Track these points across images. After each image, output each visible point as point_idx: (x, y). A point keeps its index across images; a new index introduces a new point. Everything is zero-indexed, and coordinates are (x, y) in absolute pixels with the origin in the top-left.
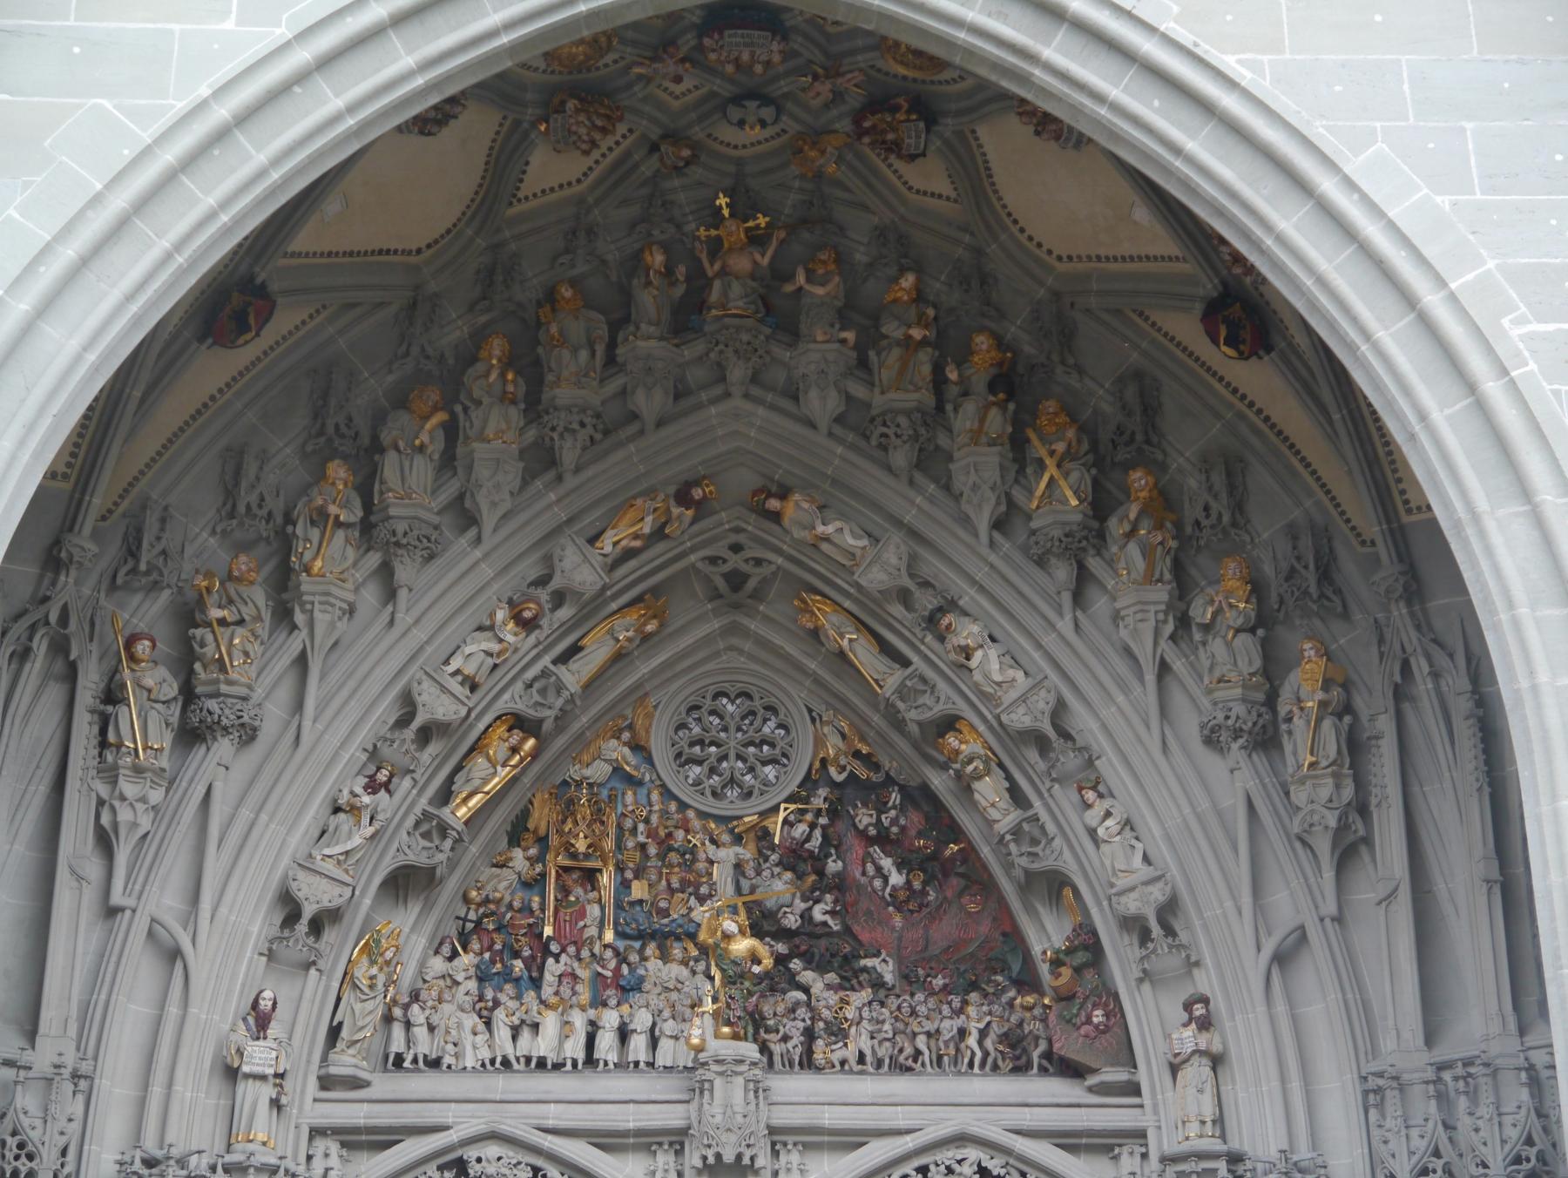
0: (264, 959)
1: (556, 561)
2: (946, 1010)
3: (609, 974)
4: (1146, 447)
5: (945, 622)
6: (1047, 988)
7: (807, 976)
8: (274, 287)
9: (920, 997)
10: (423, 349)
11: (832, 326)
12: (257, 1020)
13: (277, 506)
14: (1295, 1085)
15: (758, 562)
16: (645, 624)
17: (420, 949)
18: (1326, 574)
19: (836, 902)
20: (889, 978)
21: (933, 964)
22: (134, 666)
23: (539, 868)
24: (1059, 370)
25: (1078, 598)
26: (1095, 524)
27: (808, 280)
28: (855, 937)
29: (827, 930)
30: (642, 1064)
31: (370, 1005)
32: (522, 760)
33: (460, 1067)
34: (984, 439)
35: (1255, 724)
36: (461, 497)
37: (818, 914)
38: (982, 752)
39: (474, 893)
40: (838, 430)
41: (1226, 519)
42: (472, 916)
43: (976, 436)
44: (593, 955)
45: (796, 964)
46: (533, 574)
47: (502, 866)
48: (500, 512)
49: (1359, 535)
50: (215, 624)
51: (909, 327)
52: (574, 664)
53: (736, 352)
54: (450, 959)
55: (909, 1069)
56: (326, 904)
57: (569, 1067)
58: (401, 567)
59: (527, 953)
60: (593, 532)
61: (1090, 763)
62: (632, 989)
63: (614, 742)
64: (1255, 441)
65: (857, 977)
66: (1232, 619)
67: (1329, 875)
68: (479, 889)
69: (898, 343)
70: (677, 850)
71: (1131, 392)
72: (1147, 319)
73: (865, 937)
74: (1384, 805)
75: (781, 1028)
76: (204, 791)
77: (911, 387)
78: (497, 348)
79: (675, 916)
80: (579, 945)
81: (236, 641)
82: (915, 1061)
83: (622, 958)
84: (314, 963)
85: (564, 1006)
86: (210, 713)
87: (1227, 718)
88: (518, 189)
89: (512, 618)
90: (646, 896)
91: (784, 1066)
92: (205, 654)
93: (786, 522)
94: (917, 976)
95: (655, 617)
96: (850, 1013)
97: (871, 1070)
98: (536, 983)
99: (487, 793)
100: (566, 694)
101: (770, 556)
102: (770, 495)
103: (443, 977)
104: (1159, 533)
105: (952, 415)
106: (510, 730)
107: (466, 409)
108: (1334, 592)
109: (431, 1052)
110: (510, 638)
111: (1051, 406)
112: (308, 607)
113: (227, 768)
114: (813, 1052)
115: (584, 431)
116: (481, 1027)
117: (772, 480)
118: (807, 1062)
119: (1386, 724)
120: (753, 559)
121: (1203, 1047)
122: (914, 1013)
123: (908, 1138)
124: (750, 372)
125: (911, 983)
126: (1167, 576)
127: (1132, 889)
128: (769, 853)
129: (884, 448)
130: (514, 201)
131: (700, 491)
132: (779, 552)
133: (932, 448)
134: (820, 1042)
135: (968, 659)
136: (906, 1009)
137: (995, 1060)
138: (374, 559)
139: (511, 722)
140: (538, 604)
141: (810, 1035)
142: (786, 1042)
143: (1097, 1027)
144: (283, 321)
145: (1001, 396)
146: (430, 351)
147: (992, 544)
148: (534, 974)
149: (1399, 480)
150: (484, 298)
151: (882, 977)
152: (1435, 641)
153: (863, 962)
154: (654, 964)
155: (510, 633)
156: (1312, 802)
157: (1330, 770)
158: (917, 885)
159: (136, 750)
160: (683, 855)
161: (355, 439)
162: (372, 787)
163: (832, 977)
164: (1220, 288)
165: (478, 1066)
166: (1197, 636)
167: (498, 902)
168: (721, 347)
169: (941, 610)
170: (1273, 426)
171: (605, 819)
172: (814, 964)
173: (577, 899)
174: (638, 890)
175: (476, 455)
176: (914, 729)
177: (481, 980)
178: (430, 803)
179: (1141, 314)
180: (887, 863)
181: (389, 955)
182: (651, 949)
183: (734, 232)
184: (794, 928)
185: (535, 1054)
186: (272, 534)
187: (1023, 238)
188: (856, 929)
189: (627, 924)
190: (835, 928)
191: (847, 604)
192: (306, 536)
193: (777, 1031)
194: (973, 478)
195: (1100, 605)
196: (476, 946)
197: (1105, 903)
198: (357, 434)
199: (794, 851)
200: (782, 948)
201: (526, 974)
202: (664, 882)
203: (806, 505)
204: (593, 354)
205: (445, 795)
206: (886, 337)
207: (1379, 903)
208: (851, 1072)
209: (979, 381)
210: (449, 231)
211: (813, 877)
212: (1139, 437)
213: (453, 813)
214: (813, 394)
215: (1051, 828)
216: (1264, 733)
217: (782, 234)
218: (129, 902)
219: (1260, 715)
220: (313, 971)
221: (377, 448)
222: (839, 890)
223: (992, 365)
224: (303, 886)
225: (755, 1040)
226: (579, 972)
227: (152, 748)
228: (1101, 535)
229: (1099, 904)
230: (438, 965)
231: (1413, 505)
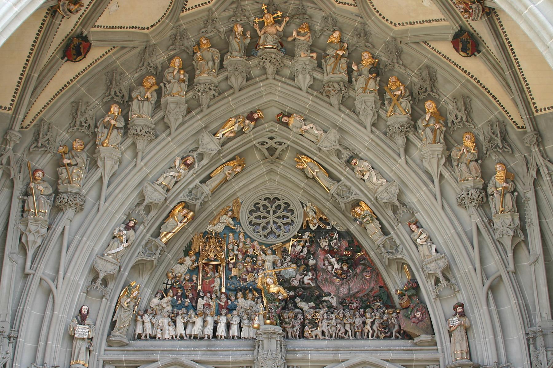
0: (85, 294)
1: (200, 140)
2: (357, 315)
3: (223, 304)
4: (431, 93)
5: (354, 161)
6: (398, 306)
7: (302, 304)
8: (91, 38)
9: (347, 310)
10: (149, 64)
11: (307, 51)
12: (81, 318)
13: (92, 123)
14: (500, 337)
15: (280, 143)
16: (236, 168)
17: (148, 294)
18: (504, 139)
19: (313, 275)
20: (334, 304)
21: (352, 299)
22: (35, 181)
23: (196, 264)
24: (397, 65)
25: (406, 151)
26: (413, 123)
27: (298, 35)
30: (235, 337)
31: (126, 314)
32: (188, 220)
33: (163, 339)
34: (367, 91)
35: (479, 196)
36: (163, 118)
37: (306, 280)
38: (370, 214)
39: (170, 274)
40: (310, 90)
41: (464, 119)
42: (170, 282)
43: (364, 90)
44: (217, 297)
45: (298, 300)
46: (191, 148)
47: (181, 264)
48: (178, 124)
49: (517, 124)
50: (67, 165)
51: (338, 50)
52: (208, 182)
53: (270, 61)
54: (161, 299)
55: (343, 338)
56: (108, 273)
57: (206, 338)
58: (140, 144)
59: (191, 296)
60: (215, 132)
61: (413, 214)
62: (233, 310)
63: (225, 217)
64: (475, 91)
65: (322, 304)
66: (469, 157)
67: (510, 255)
68: (172, 273)
69: (333, 57)
70: (250, 256)
71: (425, 73)
72: (430, 46)
73: (325, 289)
74: (532, 226)
75: (291, 322)
76: (62, 229)
77: (338, 72)
78: (177, 62)
79: (249, 282)
80: (211, 293)
81: (75, 171)
82: (345, 335)
83: (228, 298)
84: (104, 296)
85: (204, 315)
86: (64, 199)
87: (468, 194)
88: (186, 5)
89: (183, 163)
90: (238, 274)
91: (292, 337)
92: (62, 176)
93: (290, 126)
94: (345, 303)
95: (240, 165)
96: (319, 316)
97: (327, 338)
98: (195, 308)
99: (174, 232)
100: (205, 195)
101: (285, 141)
102: (284, 116)
103: (158, 305)
104: (438, 124)
105: (355, 82)
106: (183, 208)
107: (165, 85)
108: (508, 145)
109: (152, 333)
110: (182, 171)
111: (393, 79)
112: (103, 159)
113: (71, 221)
114: (304, 332)
115: (211, 92)
116: (172, 323)
117: (285, 111)
118: (302, 336)
119: (531, 195)
120: (278, 142)
121: (462, 323)
122: (344, 316)
123: (343, 364)
124: (276, 69)
125: (343, 306)
126: (442, 141)
127: (432, 262)
128: (286, 257)
129: (328, 96)
130: (185, 10)
131: (257, 115)
132: (288, 139)
133: (347, 96)
134: (307, 329)
135: (363, 176)
136: (341, 315)
137: (378, 333)
138: (129, 141)
139: (184, 205)
140: (194, 158)
141: (303, 325)
142: (293, 328)
143: (418, 319)
144: (94, 54)
145: (374, 75)
146: (152, 65)
147: (372, 131)
148: (194, 304)
149: (533, 99)
150: (173, 45)
151: (332, 304)
152: (549, 161)
153: (324, 299)
154: (241, 301)
155: (182, 169)
156: (503, 226)
157: (509, 213)
158: (345, 268)
159: (35, 213)
160: (252, 259)
161: (122, 98)
162: (128, 228)
163: (312, 304)
164: (459, 28)
165: (170, 338)
166: (455, 164)
167: (180, 277)
168: (264, 60)
169: (352, 158)
170: (481, 84)
171: (222, 245)
172: (305, 299)
173: (211, 276)
174: (234, 272)
175: (168, 101)
176: (343, 206)
177: (173, 307)
178: (151, 236)
179: (428, 44)
180: (333, 260)
181: (135, 294)
182: (240, 294)
183: (269, 18)
184: (296, 285)
185: (193, 333)
186: (90, 133)
187: (380, 18)
188: (321, 285)
189: (230, 285)
190: (313, 285)
191: (315, 158)
192: (102, 132)
193: (290, 324)
194: (364, 105)
195: (415, 153)
196: (170, 293)
197: (420, 270)
198: (123, 95)
199: (296, 256)
200: (292, 293)
201: (190, 304)
202: (245, 269)
203: (298, 119)
204: (215, 64)
205: (157, 234)
206: (329, 55)
207: (531, 265)
208: (320, 339)
209: (365, 70)
210: (159, 21)
211: (304, 266)
212: (429, 89)
213: (160, 240)
214: (300, 76)
215: (398, 241)
216: (482, 201)
217: (288, 19)
218: (33, 272)
219: (481, 193)
220: (104, 299)
221: (131, 99)
222: (314, 271)
223: (370, 64)
224: (100, 267)
225: (281, 325)
226: (211, 303)
227: (41, 212)
228: (415, 128)
229: (418, 270)
230: (156, 301)
231: (538, 108)
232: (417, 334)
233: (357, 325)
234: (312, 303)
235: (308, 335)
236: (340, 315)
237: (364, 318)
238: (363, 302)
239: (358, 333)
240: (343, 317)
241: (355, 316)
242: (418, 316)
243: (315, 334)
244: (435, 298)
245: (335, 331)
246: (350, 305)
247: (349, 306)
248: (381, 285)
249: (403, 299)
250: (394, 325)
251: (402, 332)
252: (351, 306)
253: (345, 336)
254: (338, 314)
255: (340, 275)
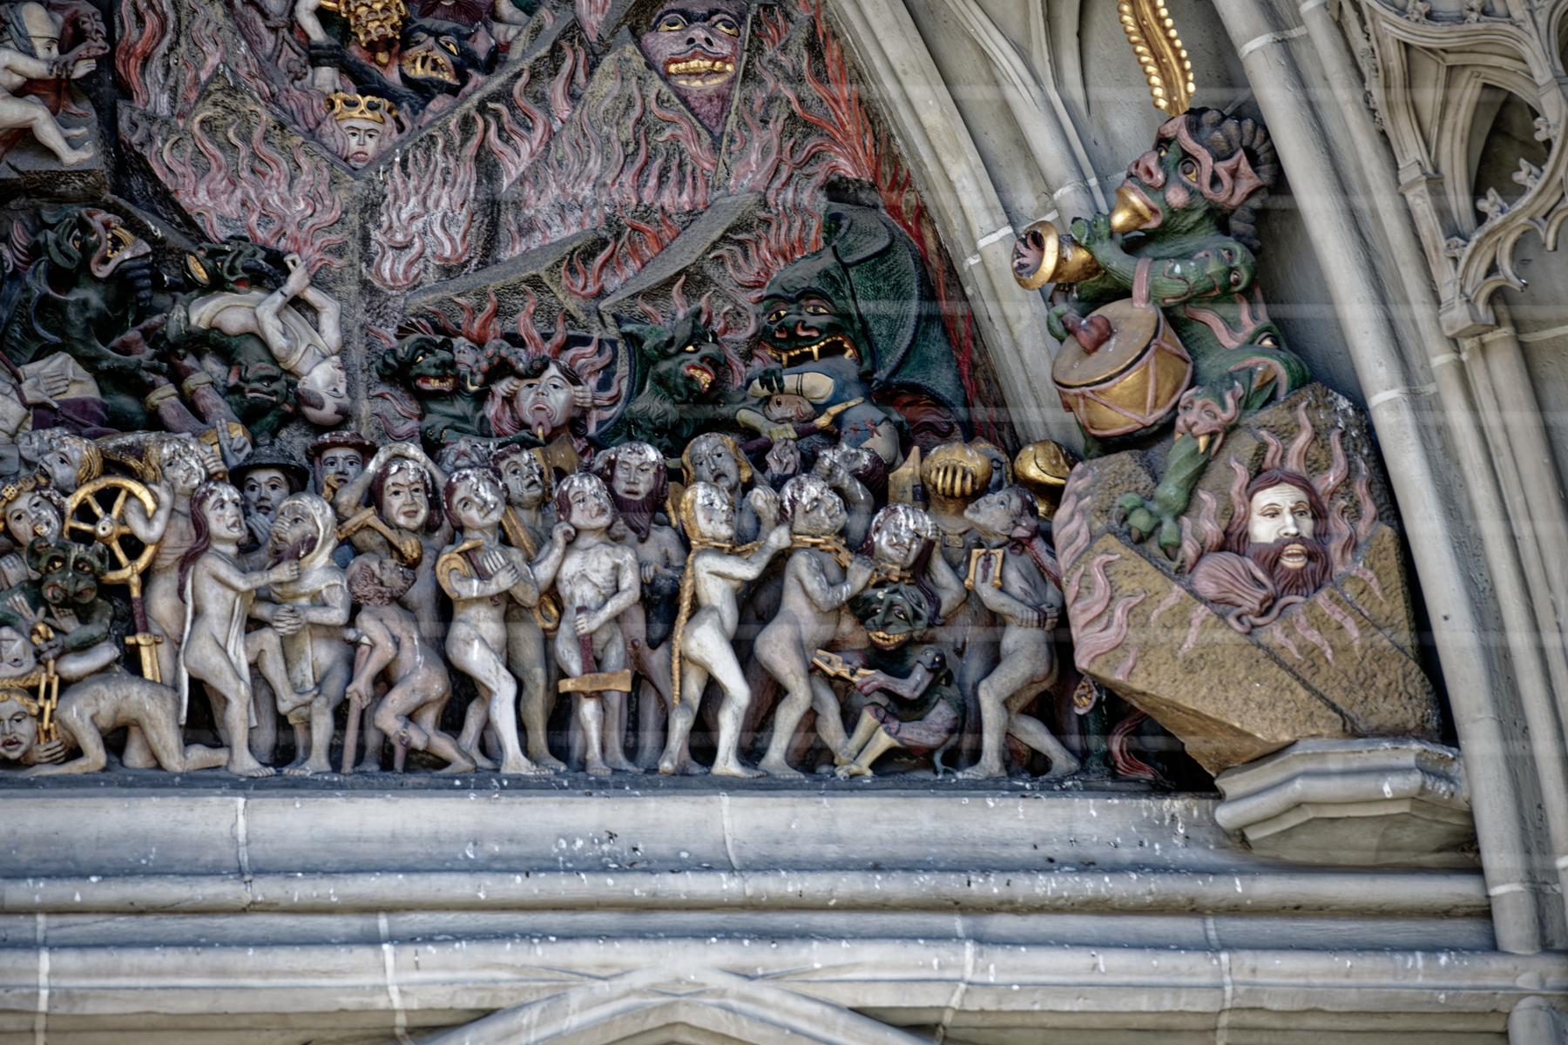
19: (71, 37)
20: (320, 378)
28: (164, 200)
29: (29, 163)
65: (177, 377)
94: (447, 368)
125: (423, 398)
151: (292, 376)
153: (203, 313)
188: (165, 159)
190: (70, 157)
232: (1266, 731)
233: (586, 624)
234: (61, 363)
235: (25, 729)
236: (396, 504)
237: (664, 538)
238: (645, 361)
239: (589, 709)
240: (429, 528)
241: (565, 507)
242: (1264, 531)
243: (105, 721)
244: (1477, 331)
245: (333, 687)
246: (502, 387)
247: (481, 398)
248: (847, 168)
249: (1107, 333)
250: (996, 620)
251: (1083, 704)
252: (509, 400)
253: (444, 746)
254: (374, 496)
255: (386, 44)
